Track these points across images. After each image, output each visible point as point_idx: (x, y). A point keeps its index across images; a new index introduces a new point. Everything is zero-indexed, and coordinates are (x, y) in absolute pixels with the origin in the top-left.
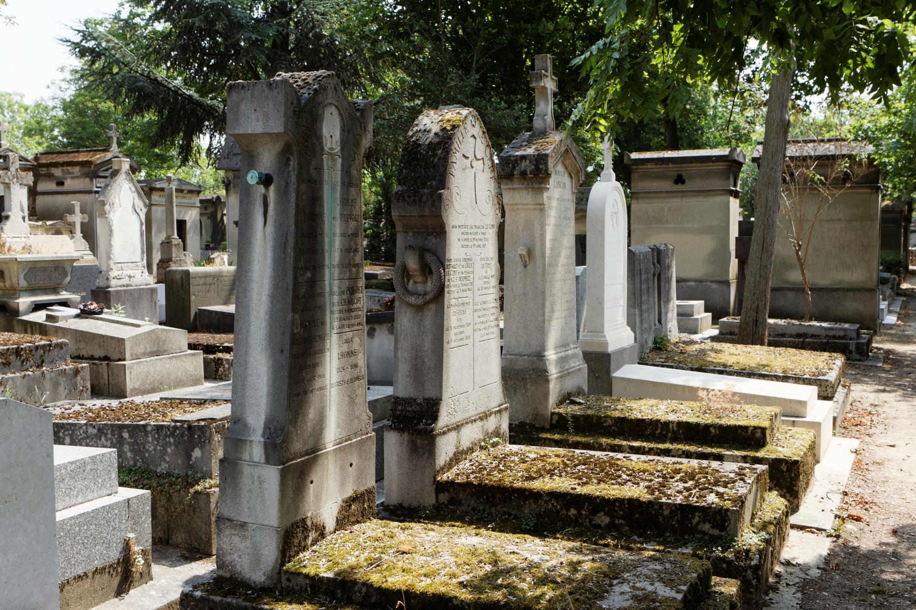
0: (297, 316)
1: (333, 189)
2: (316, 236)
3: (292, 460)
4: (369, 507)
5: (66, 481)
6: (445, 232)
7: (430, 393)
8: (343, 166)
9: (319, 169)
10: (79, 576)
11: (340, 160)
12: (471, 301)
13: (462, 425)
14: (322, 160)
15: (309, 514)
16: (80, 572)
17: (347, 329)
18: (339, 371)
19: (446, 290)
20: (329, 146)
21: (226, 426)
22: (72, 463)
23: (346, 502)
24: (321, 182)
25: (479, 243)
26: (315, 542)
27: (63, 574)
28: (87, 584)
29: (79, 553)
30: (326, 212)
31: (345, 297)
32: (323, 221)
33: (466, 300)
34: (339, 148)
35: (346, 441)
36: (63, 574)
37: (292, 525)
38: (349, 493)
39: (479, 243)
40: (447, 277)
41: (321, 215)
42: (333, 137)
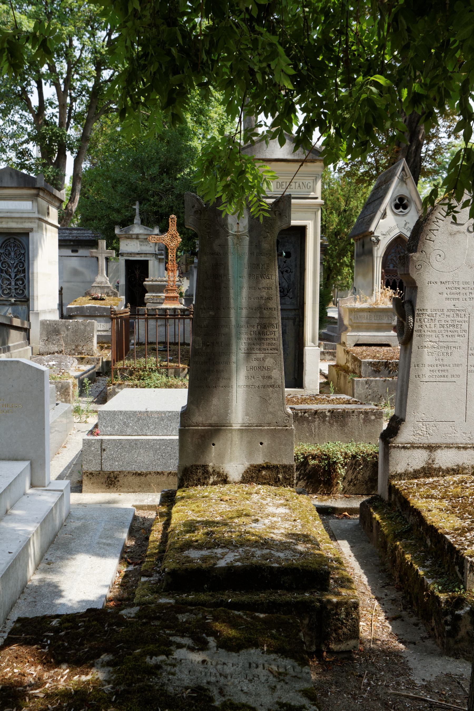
0: (199, 338)
1: (240, 257)
2: (220, 289)
3: (194, 426)
4: (285, 478)
5: (165, 420)
6: (417, 287)
7: (403, 417)
8: (251, 242)
9: (224, 246)
10: (158, 473)
11: (248, 238)
12: (465, 346)
13: (439, 447)
14: (227, 240)
15: (211, 464)
16: (159, 470)
17: (258, 352)
18: (247, 377)
19: (415, 333)
20: (235, 229)
21: (300, 414)
22: (170, 412)
23: (255, 467)
24: (226, 253)
25: (456, 296)
26: (214, 483)
27: (147, 468)
28: (164, 478)
29: (159, 459)
30: (230, 272)
31: (255, 329)
32: (228, 280)
33: (457, 345)
34: (247, 230)
35: (257, 426)
36: (147, 468)
37: (192, 466)
38: (260, 460)
39: (456, 296)
40: (416, 325)
41: (226, 275)
42: (240, 224)
